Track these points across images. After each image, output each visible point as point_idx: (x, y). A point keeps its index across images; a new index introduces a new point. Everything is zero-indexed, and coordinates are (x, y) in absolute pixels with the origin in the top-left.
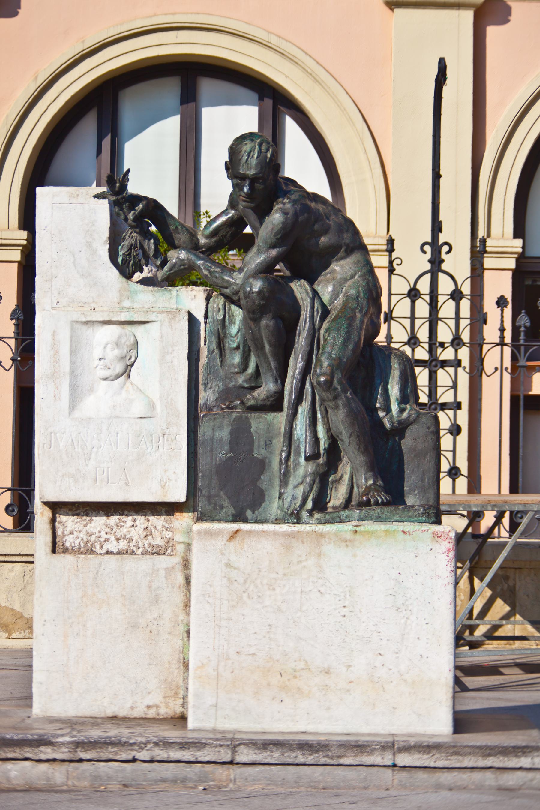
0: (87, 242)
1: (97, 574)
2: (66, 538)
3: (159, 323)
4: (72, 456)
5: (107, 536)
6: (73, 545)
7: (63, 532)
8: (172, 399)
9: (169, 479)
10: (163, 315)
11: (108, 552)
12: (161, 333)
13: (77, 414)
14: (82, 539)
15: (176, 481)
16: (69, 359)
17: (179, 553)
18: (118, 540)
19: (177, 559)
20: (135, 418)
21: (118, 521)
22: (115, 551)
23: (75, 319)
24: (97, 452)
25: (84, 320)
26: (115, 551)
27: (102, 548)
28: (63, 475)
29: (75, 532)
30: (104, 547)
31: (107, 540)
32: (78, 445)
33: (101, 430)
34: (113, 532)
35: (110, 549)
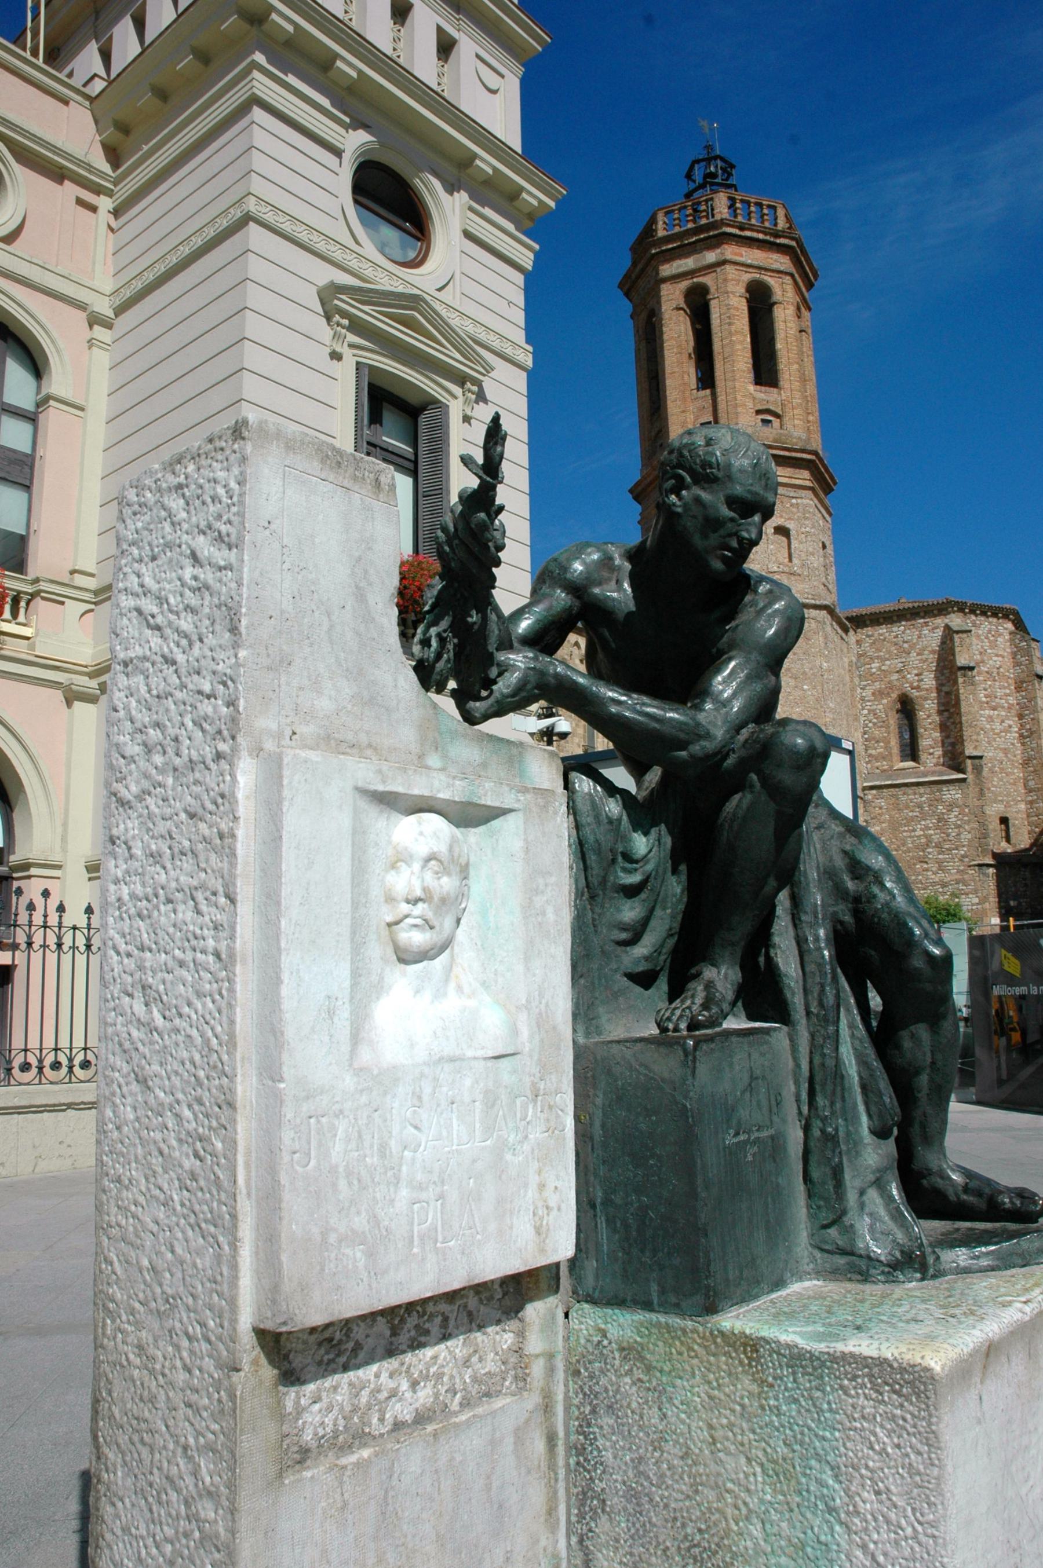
0: (357, 587)
1: (385, 1498)
2: (307, 1417)
3: (520, 814)
4: (359, 1181)
5: (392, 1384)
6: (321, 1432)
7: (297, 1402)
8: (547, 1005)
9: (547, 1208)
10: (529, 796)
11: (398, 1426)
12: (526, 840)
13: (365, 1056)
14: (342, 1409)
15: (559, 1209)
16: (349, 896)
17: (535, 1384)
18: (414, 1385)
19: (532, 1400)
20: (485, 1059)
21: (413, 1333)
22: (409, 1418)
23: (360, 784)
24: (413, 1159)
25: (381, 788)
26: (409, 1418)
27: (382, 1420)
28: (340, 1241)
29: (324, 1394)
30: (387, 1416)
31: (393, 1394)
32: (372, 1146)
33: (420, 1098)
34: (404, 1368)
35: (400, 1417)
